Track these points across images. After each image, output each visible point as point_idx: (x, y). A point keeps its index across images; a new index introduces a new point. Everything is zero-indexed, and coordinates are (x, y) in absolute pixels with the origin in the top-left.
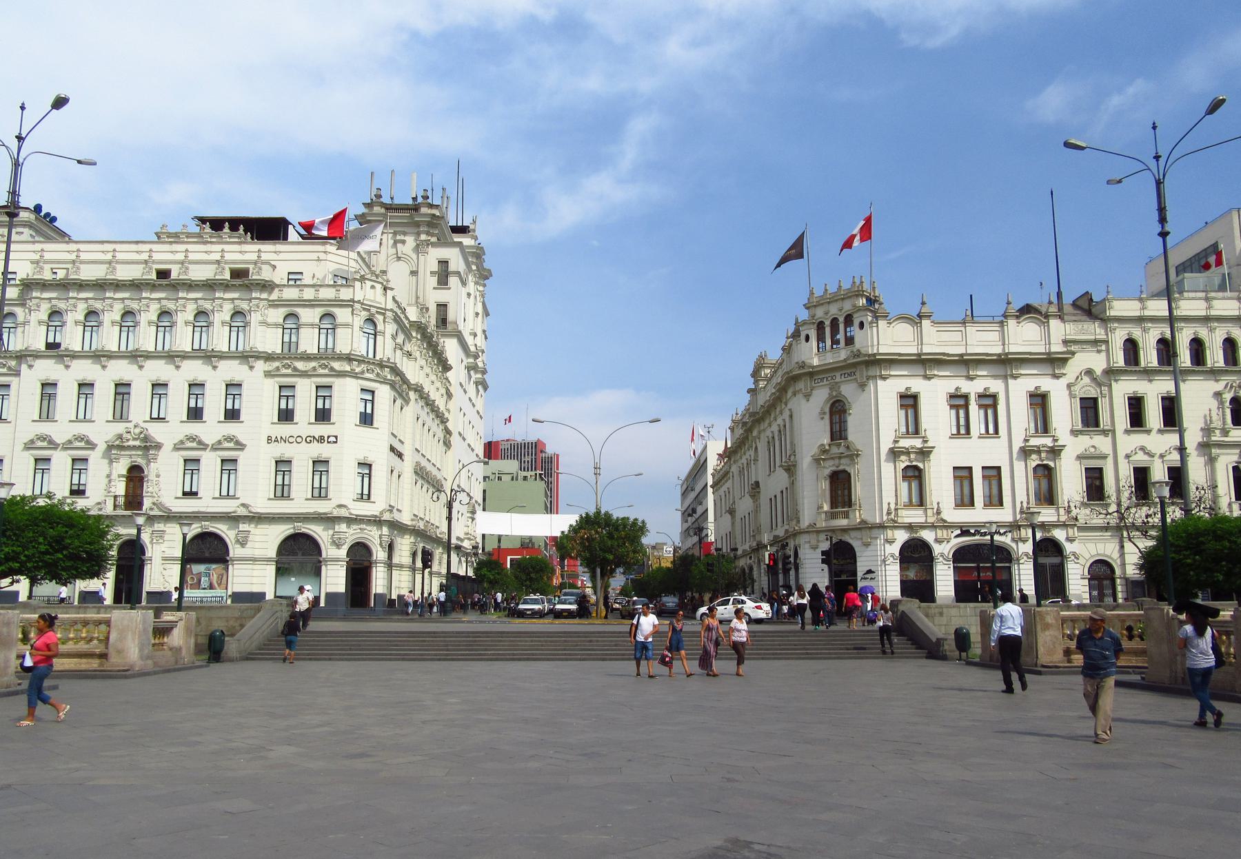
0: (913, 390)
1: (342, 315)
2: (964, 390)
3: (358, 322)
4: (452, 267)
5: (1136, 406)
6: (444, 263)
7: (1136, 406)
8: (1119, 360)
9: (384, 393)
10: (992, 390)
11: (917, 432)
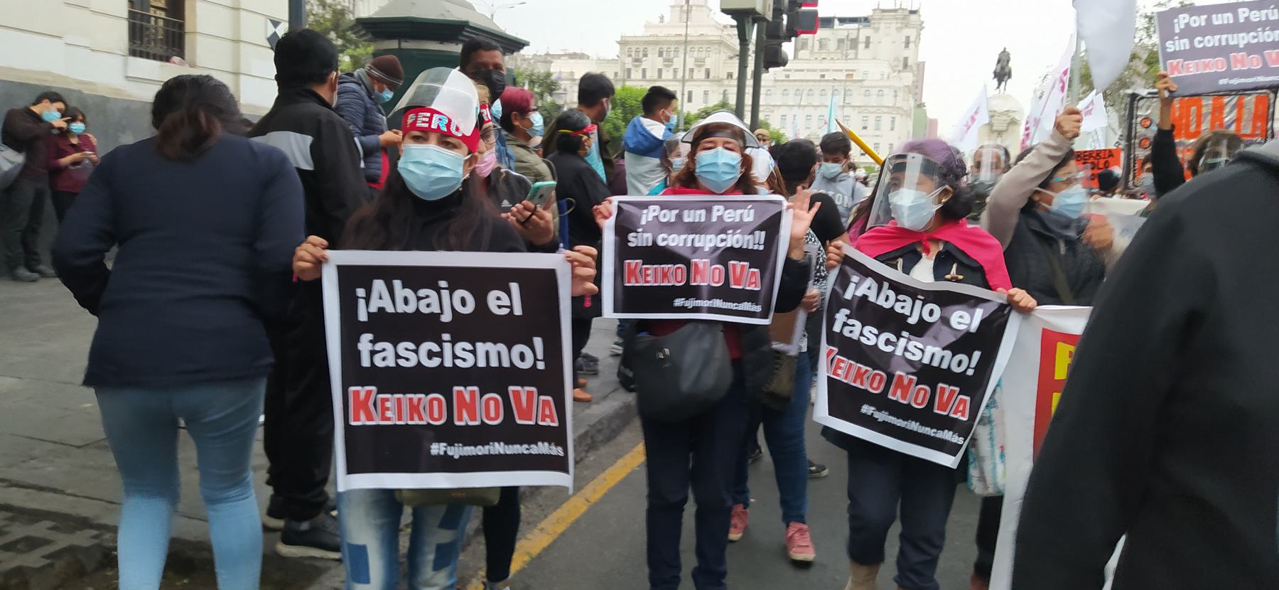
1: (886, 91)
3: (892, 93)
4: (912, 39)
6: (908, 38)
9: (898, 118)
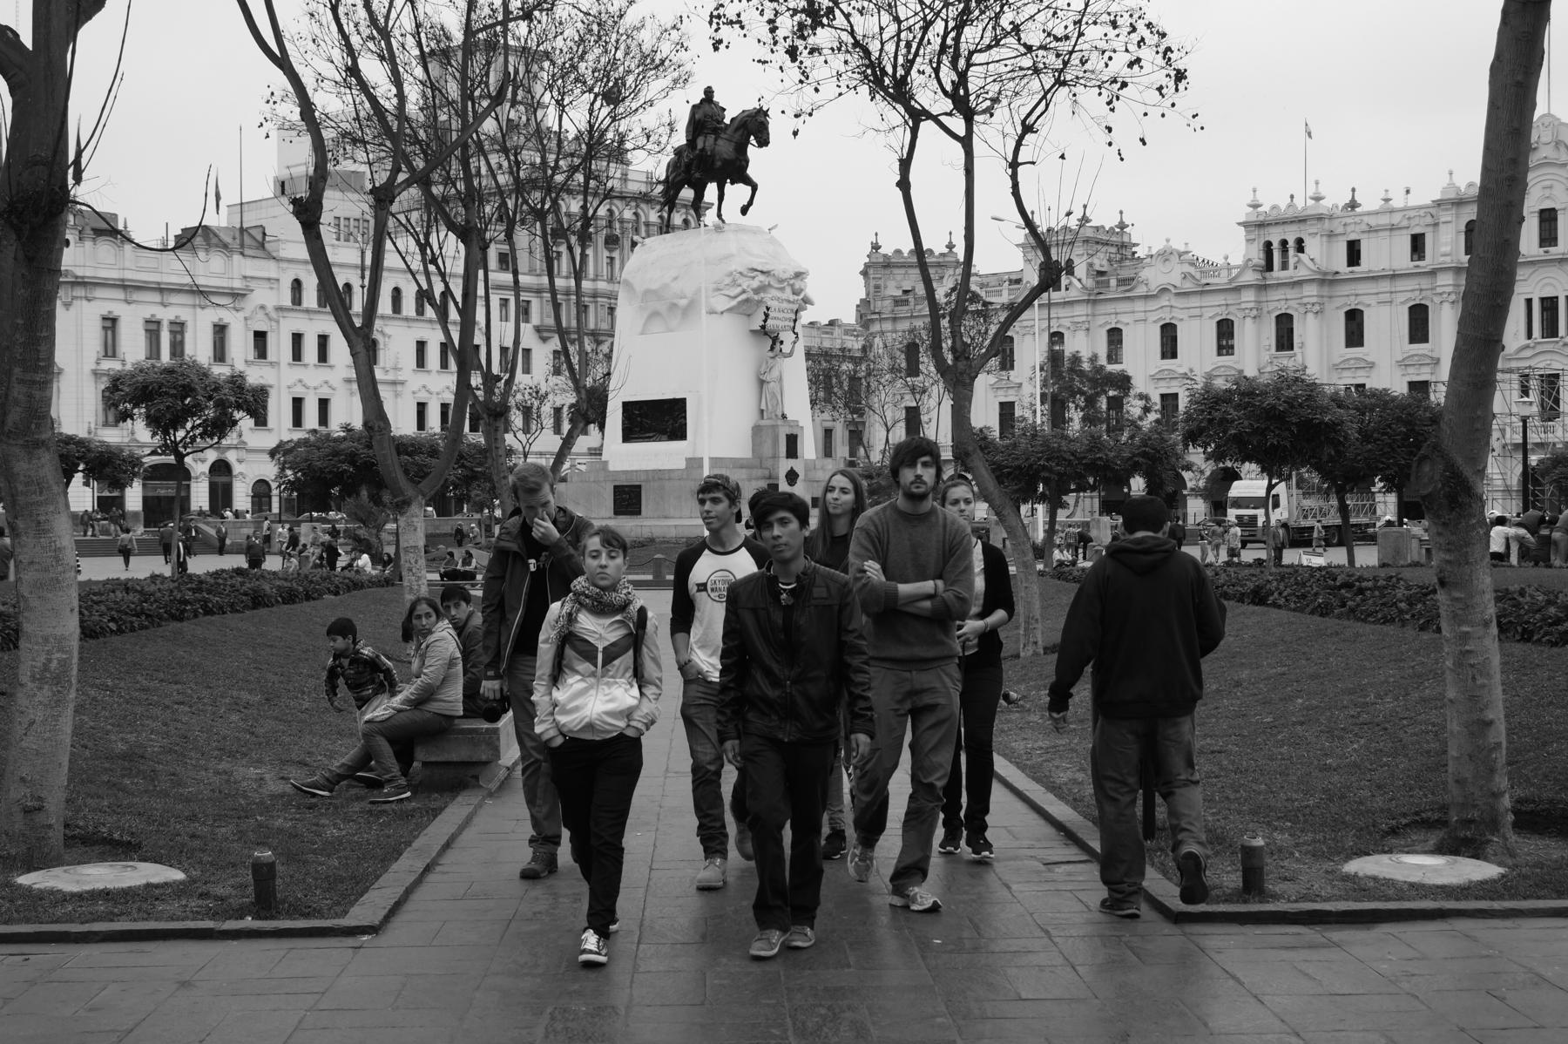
0: (116, 313)
2: (158, 317)
5: (297, 339)
7: (297, 339)
8: (288, 302)
10: (183, 318)
11: (114, 356)
